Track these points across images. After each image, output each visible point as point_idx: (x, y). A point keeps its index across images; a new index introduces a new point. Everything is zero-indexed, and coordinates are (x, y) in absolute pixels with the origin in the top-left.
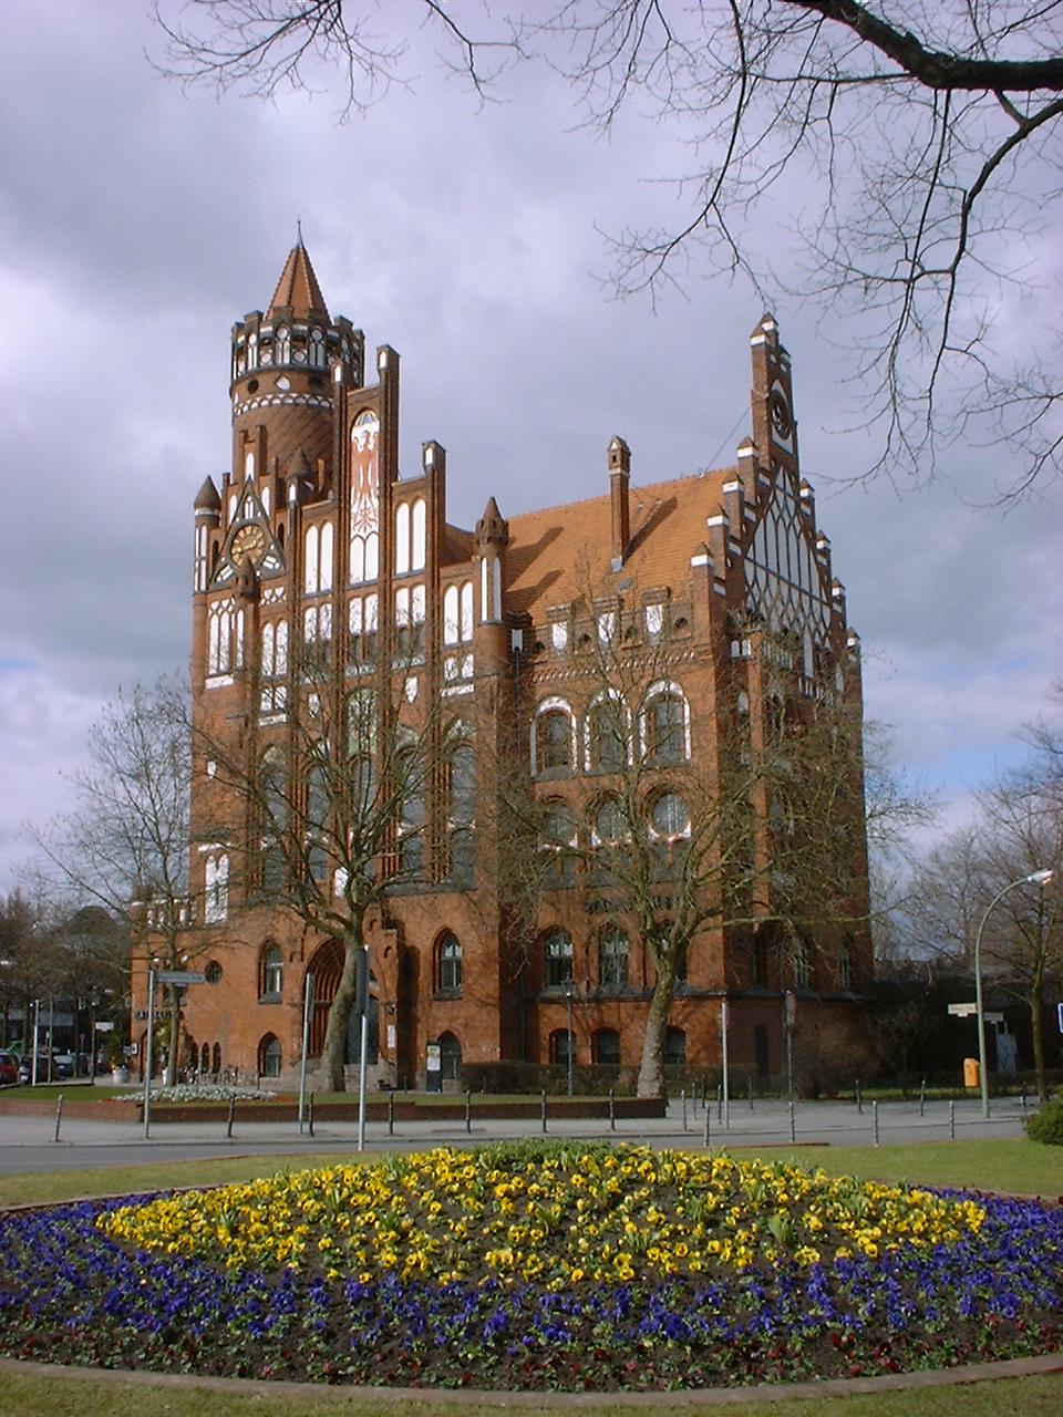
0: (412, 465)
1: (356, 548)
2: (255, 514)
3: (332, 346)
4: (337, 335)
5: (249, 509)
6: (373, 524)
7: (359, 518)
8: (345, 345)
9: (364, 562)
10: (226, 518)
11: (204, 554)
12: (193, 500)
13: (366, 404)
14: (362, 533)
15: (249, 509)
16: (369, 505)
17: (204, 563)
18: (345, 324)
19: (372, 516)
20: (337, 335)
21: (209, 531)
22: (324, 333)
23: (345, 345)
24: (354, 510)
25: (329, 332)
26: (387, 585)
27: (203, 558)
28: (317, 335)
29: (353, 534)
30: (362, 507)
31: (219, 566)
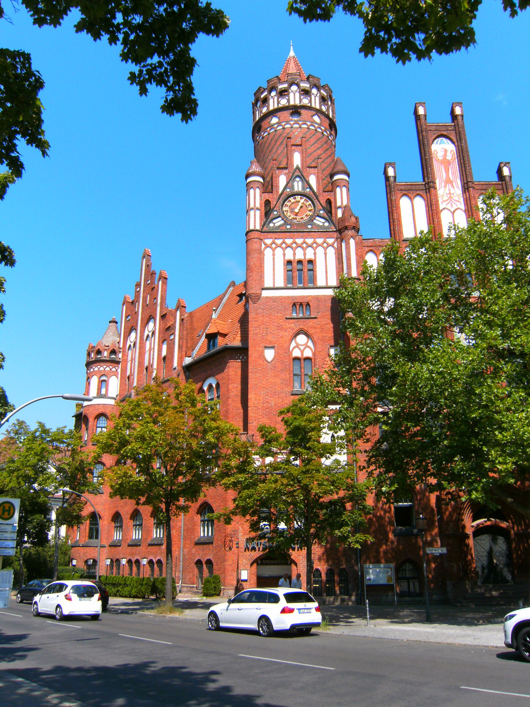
2: (303, 188)
6: (458, 204)
7: (445, 198)
10: (278, 187)
11: (258, 205)
14: (449, 207)
19: (456, 198)
28: (314, 91)
29: (441, 207)
31: (271, 216)
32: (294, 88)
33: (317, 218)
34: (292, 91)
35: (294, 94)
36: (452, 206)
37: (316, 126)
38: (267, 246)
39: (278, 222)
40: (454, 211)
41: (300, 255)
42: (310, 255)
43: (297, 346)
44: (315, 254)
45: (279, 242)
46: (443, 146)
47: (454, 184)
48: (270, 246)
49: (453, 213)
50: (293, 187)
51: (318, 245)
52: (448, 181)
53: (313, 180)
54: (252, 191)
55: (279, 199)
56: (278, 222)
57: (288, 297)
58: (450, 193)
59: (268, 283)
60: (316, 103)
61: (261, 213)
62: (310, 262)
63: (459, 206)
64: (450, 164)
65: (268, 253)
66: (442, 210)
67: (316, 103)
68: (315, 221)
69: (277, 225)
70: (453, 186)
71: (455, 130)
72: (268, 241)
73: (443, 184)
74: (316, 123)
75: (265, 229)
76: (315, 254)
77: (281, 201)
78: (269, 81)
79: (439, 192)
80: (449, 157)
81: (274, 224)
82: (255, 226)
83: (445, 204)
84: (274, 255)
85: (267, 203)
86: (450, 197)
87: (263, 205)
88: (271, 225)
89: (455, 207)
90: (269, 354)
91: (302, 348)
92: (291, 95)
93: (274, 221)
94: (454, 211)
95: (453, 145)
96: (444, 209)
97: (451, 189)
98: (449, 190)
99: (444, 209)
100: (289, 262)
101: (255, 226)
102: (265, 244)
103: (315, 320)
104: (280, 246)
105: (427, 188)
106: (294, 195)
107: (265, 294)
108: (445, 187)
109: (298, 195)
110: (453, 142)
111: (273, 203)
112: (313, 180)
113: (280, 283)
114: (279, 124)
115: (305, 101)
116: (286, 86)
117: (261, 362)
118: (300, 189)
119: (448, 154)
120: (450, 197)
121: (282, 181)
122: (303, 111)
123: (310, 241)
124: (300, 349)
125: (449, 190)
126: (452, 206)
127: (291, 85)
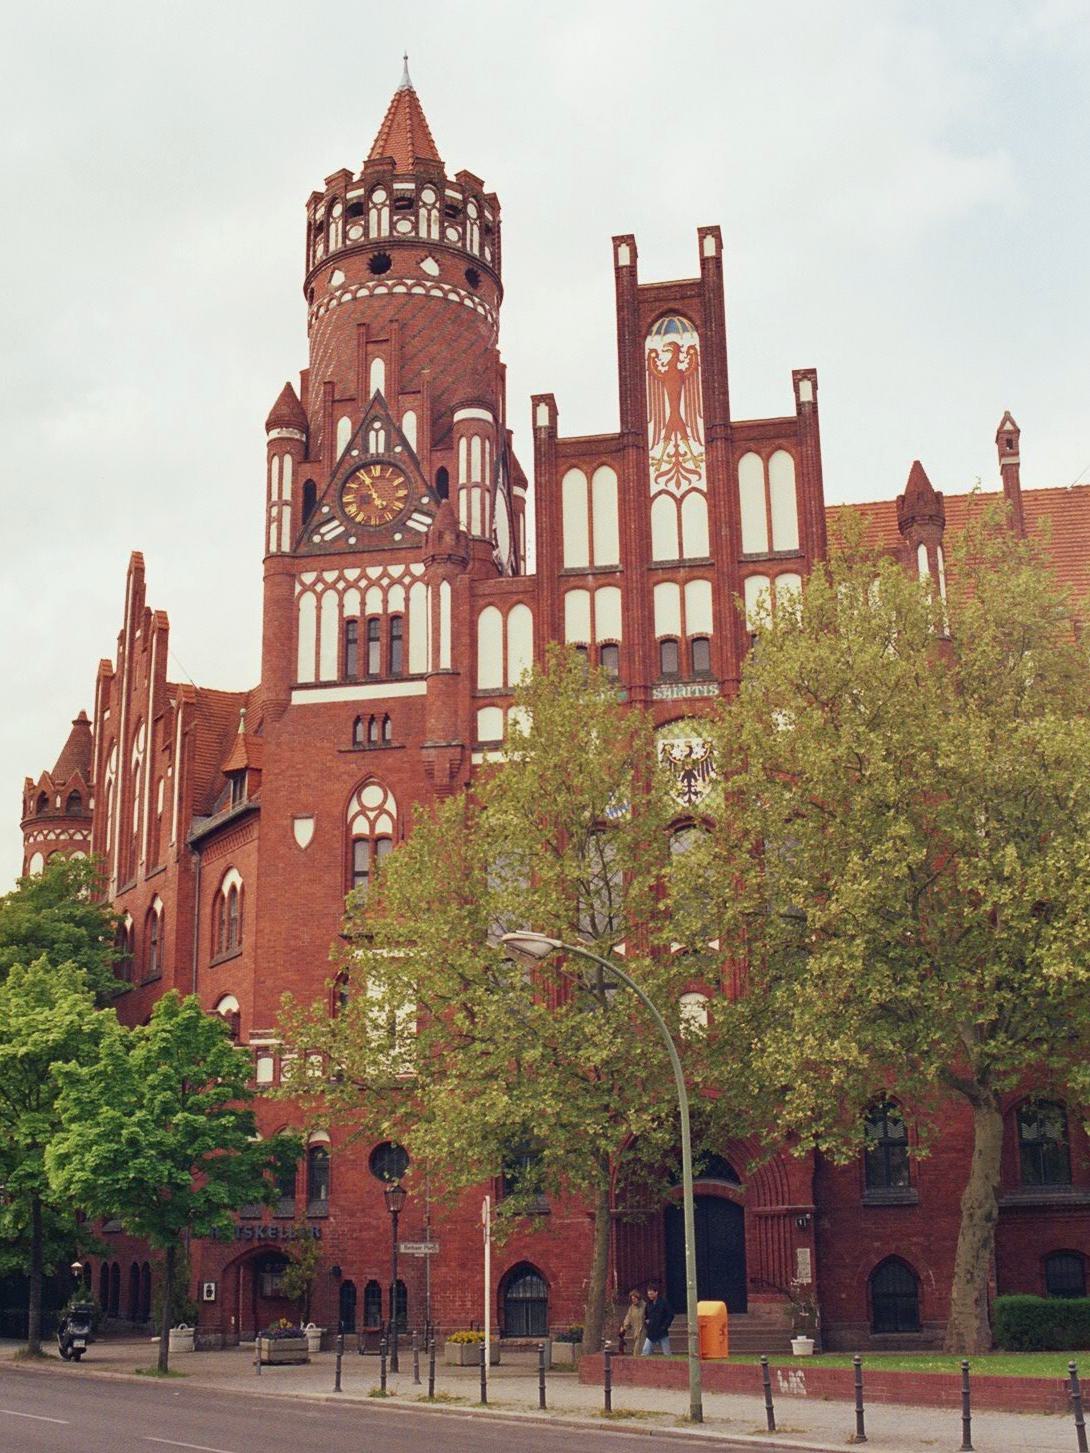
0: (757, 396)
1: (662, 513)
2: (389, 446)
3: (452, 213)
4: (459, 196)
5: (377, 442)
6: (694, 478)
7: (665, 467)
8: (472, 211)
9: (681, 528)
10: (333, 447)
11: (287, 495)
12: (265, 417)
13: (672, 305)
14: (672, 487)
15: (377, 442)
16: (683, 448)
17: (287, 511)
18: (469, 183)
19: (690, 465)
20: (459, 196)
21: (296, 465)
22: (440, 197)
23: (472, 211)
24: (656, 452)
25: (449, 192)
26: (727, 566)
27: (286, 503)
28: (428, 196)
29: (654, 489)
30: (671, 450)
32: (380, 196)
33: (416, 516)
34: (375, 205)
35: (379, 211)
36: (678, 485)
37: (429, 284)
38: (306, 589)
39: (332, 531)
40: (683, 496)
41: (374, 606)
42: (396, 605)
43: (363, 811)
44: (407, 600)
45: (330, 576)
46: (671, 337)
47: (689, 430)
48: (311, 588)
49: (679, 502)
50: (366, 449)
51: (415, 579)
52: (677, 426)
53: (410, 424)
54: (276, 460)
55: (333, 475)
56: (332, 531)
57: (346, 703)
58: (677, 454)
59: (305, 674)
60: (429, 228)
61: (293, 514)
62: (397, 618)
63: (696, 484)
65: (307, 602)
66: (656, 496)
67: (429, 228)
68: (410, 523)
69: (328, 537)
70: (685, 437)
71: (701, 302)
72: (308, 578)
73: (663, 433)
74: (428, 277)
75: (303, 550)
76: (407, 600)
77: (338, 482)
78: (329, 181)
79: (651, 454)
80: (682, 366)
81: (323, 535)
82: (279, 545)
84: (319, 608)
86: (678, 464)
87: (301, 492)
88: (317, 539)
90: (304, 832)
91: (372, 815)
92: (373, 213)
93: (323, 530)
94: (683, 496)
95: (695, 334)
97: (680, 442)
98: (676, 446)
99: (660, 493)
100: (352, 621)
101: (279, 545)
102: (302, 584)
103: (399, 754)
104: (332, 586)
105: (623, 450)
106: (366, 466)
107: (299, 698)
108: (667, 438)
109: (375, 463)
110: (697, 328)
111: (322, 487)
112: (410, 424)
113: (330, 672)
114: (344, 288)
115: (404, 227)
116: (361, 192)
117: (283, 850)
118: (381, 450)
119: (682, 356)
120: (678, 464)
121: (345, 428)
122: (395, 255)
123: (396, 571)
124: (368, 818)
125: (676, 446)
126: (678, 485)
127: (370, 191)
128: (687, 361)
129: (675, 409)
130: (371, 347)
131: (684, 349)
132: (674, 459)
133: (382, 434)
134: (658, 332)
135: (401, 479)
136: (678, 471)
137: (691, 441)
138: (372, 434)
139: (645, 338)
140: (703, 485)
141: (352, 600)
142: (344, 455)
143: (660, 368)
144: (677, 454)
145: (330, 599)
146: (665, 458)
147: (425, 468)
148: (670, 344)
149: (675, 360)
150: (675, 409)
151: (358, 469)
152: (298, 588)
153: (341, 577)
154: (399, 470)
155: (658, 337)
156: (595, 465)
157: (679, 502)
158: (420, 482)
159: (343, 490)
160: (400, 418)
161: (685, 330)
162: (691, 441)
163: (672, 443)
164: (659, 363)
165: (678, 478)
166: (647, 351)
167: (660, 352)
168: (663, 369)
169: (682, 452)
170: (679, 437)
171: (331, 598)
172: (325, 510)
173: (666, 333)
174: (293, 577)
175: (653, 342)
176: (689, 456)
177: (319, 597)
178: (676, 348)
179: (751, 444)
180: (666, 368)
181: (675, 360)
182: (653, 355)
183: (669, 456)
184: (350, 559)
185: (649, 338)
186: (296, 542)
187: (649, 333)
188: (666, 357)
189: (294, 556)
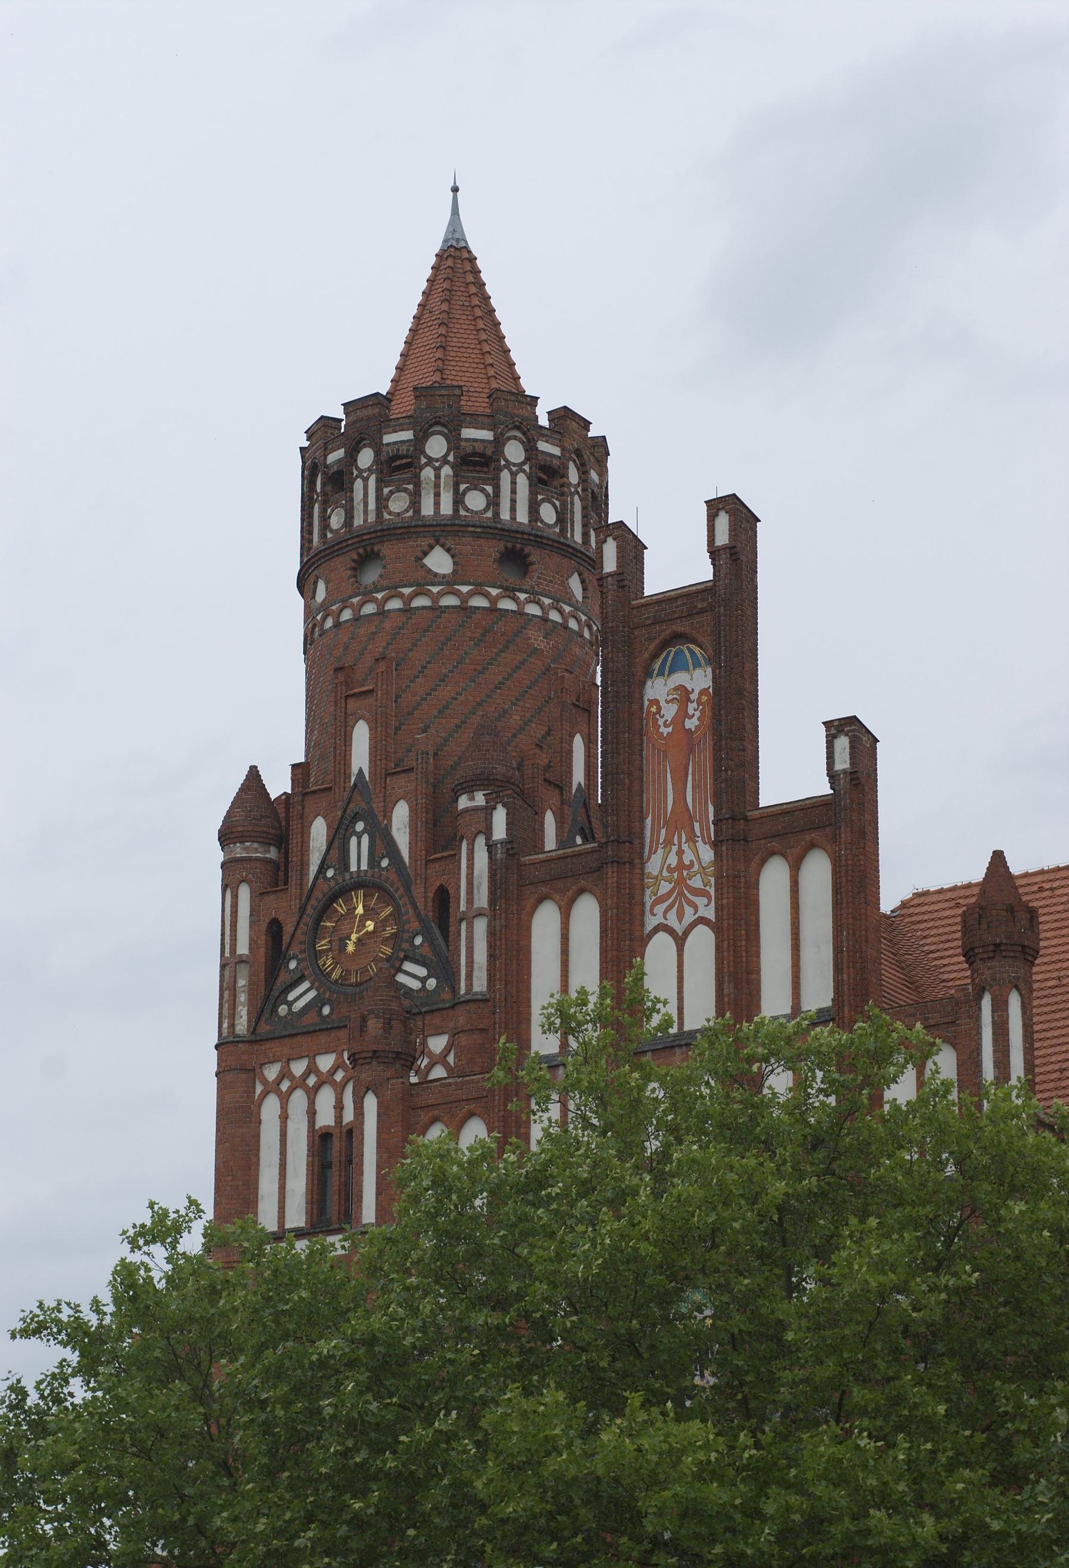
6: (700, 901)
7: (665, 887)
14: (672, 920)
19: (697, 883)
24: (654, 865)
27: (241, 960)
29: (651, 922)
30: (673, 860)
36: (680, 916)
39: (302, 996)
40: (687, 933)
45: (298, 1068)
46: (680, 678)
47: (697, 826)
48: (273, 1088)
49: (680, 941)
52: (681, 822)
64: (691, 750)
65: (270, 1108)
66: (650, 936)
70: (692, 839)
72: (272, 1072)
75: (264, 1028)
80: (691, 724)
83: (660, 909)
84: (284, 1117)
85: (275, 929)
86: (681, 882)
87: (262, 941)
88: (283, 1010)
89: (689, 916)
96: (656, 930)
97: (685, 847)
98: (680, 853)
99: (656, 930)
104: (299, 1083)
108: (669, 842)
119: (691, 707)
120: (681, 882)
125: (680, 853)
126: (680, 916)
128: (698, 714)
129: (680, 795)
130: (352, 704)
131: (694, 696)
132: (676, 875)
133: (365, 839)
134: (661, 673)
135: (389, 910)
136: (681, 894)
137: (700, 844)
138: (354, 841)
139: (643, 684)
140: (710, 914)
141: (326, 1099)
142: (316, 878)
143: (662, 729)
144: (681, 866)
145: (299, 1099)
146: (665, 873)
147: (418, 891)
148: (676, 689)
149: (683, 714)
150: (680, 795)
151: (334, 898)
152: (259, 1089)
153: (312, 1069)
154: (387, 897)
155: (659, 681)
156: (570, 894)
157: (680, 941)
158: (411, 912)
159: (316, 931)
160: (388, 814)
161: (697, 665)
162: (700, 844)
163: (675, 849)
164: (661, 722)
165: (681, 904)
166: (646, 703)
167: (662, 704)
168: (665, 731)
169: (687, 863)
170: (684, 840)
171: (299, 1099)
172: (293, 965)
173: (669, 675)
174: (252, 1073)
175: (657, 689)
176: (696, 867)
177: (284, 1099)
178: (683, 695)
179: (774, 844)
180: (670, 729)
181: (683, 714)
182: (654, 709)
183: (670, 870)
184: (322, 1038)
185: (649, 683)
186: (257, 1017)
187: (648, 674)
188: (670, 711)
189: (255, 1038)
